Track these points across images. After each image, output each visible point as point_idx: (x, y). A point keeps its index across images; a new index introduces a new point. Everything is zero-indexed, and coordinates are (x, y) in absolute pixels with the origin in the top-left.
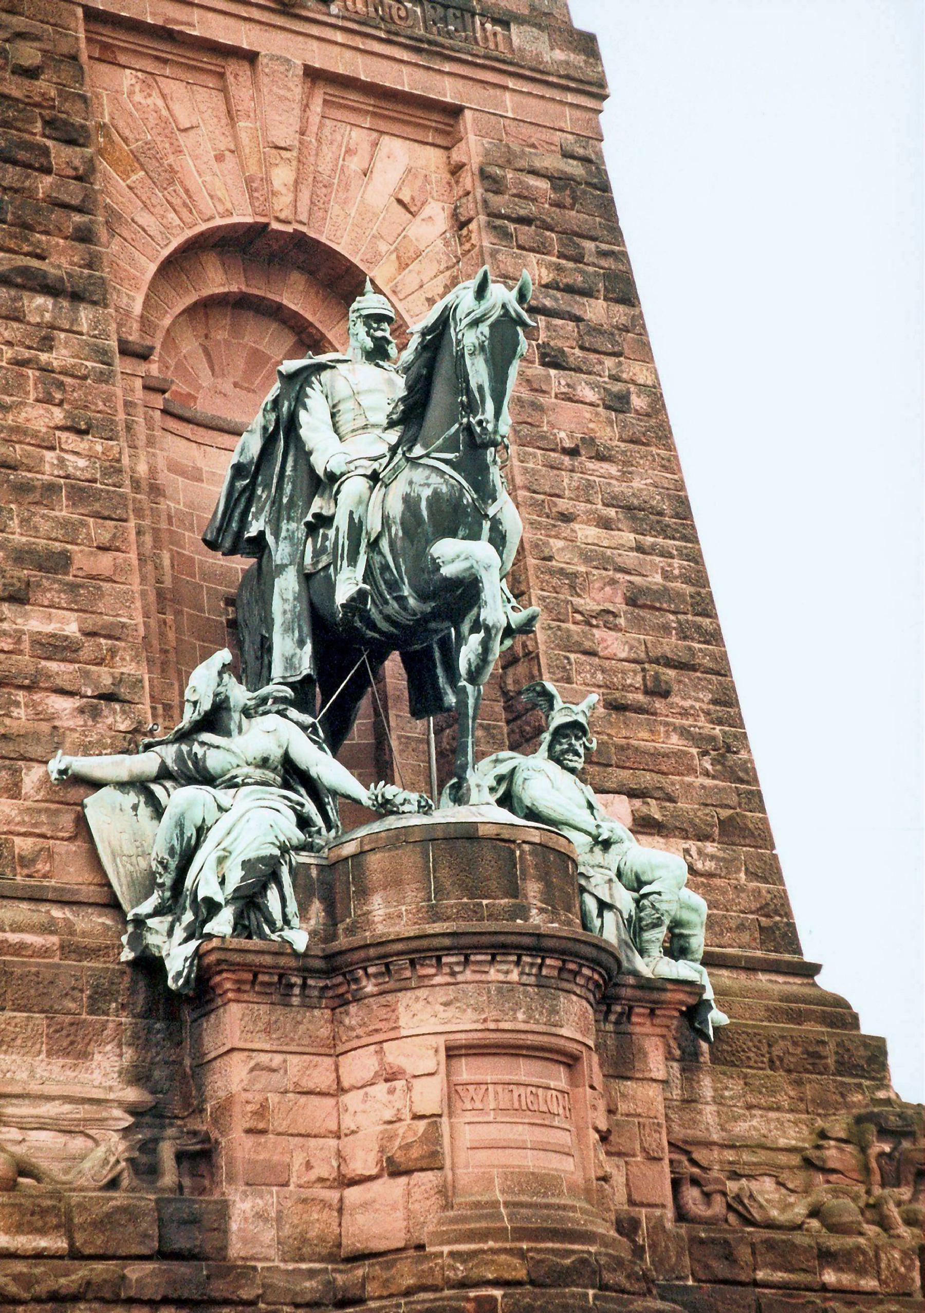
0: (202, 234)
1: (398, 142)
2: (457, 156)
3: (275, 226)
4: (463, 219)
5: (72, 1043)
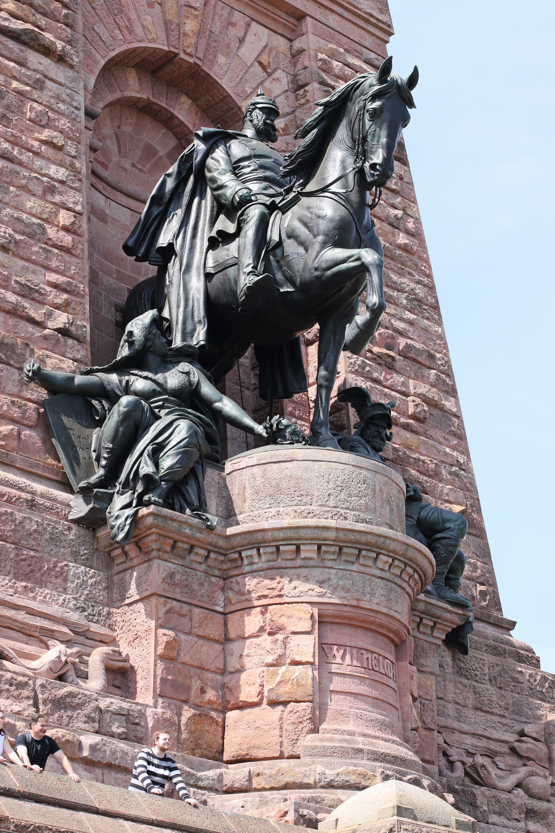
0: (135, 50)
2: (297, 44)
3: (182, 56)
4: (301, 83)
5: (32, 571)
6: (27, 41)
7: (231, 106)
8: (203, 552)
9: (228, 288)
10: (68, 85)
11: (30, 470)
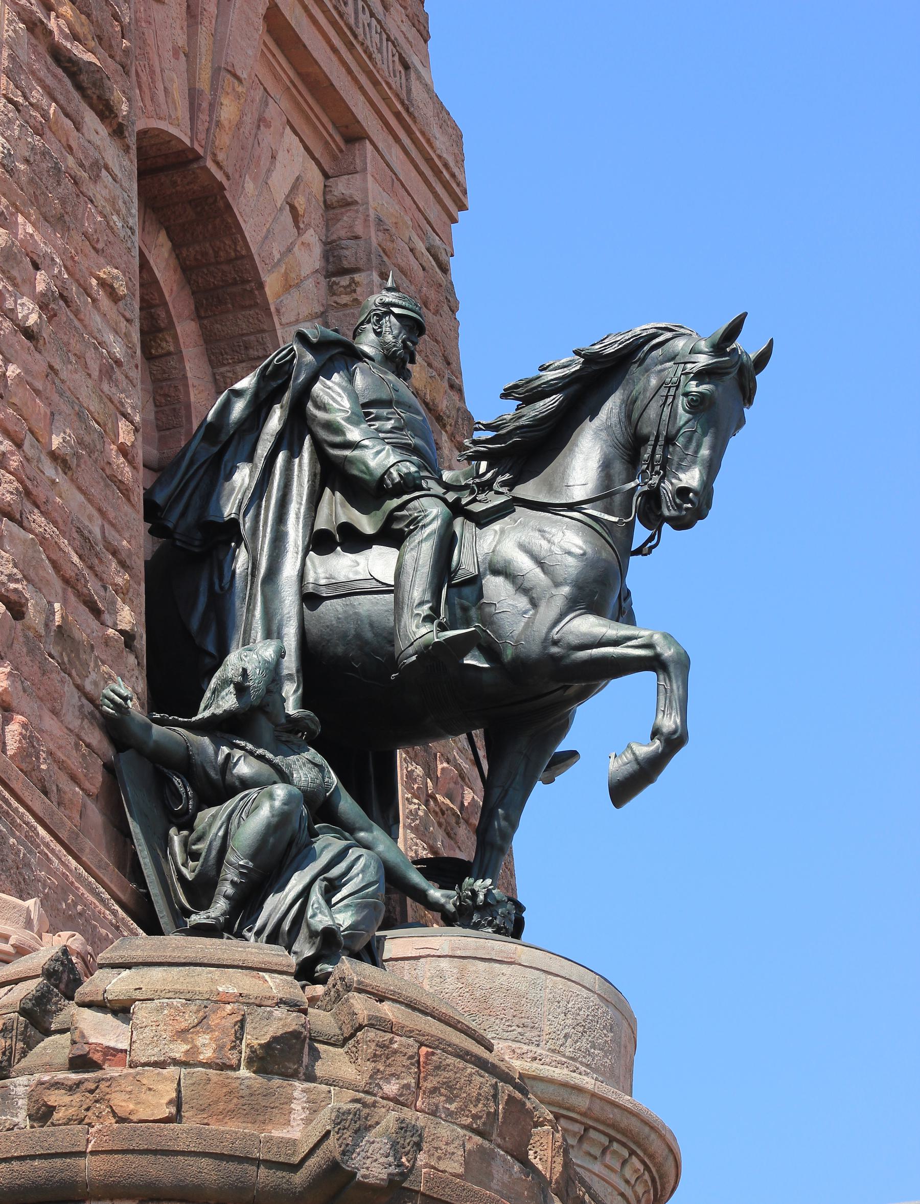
2: (342, 187)
3: (210, 164)
4: (346, 265)
6: (85, 85)
7: (246, 276)
9: (353, 632)
10: (123, 184)
11: (97, 871)
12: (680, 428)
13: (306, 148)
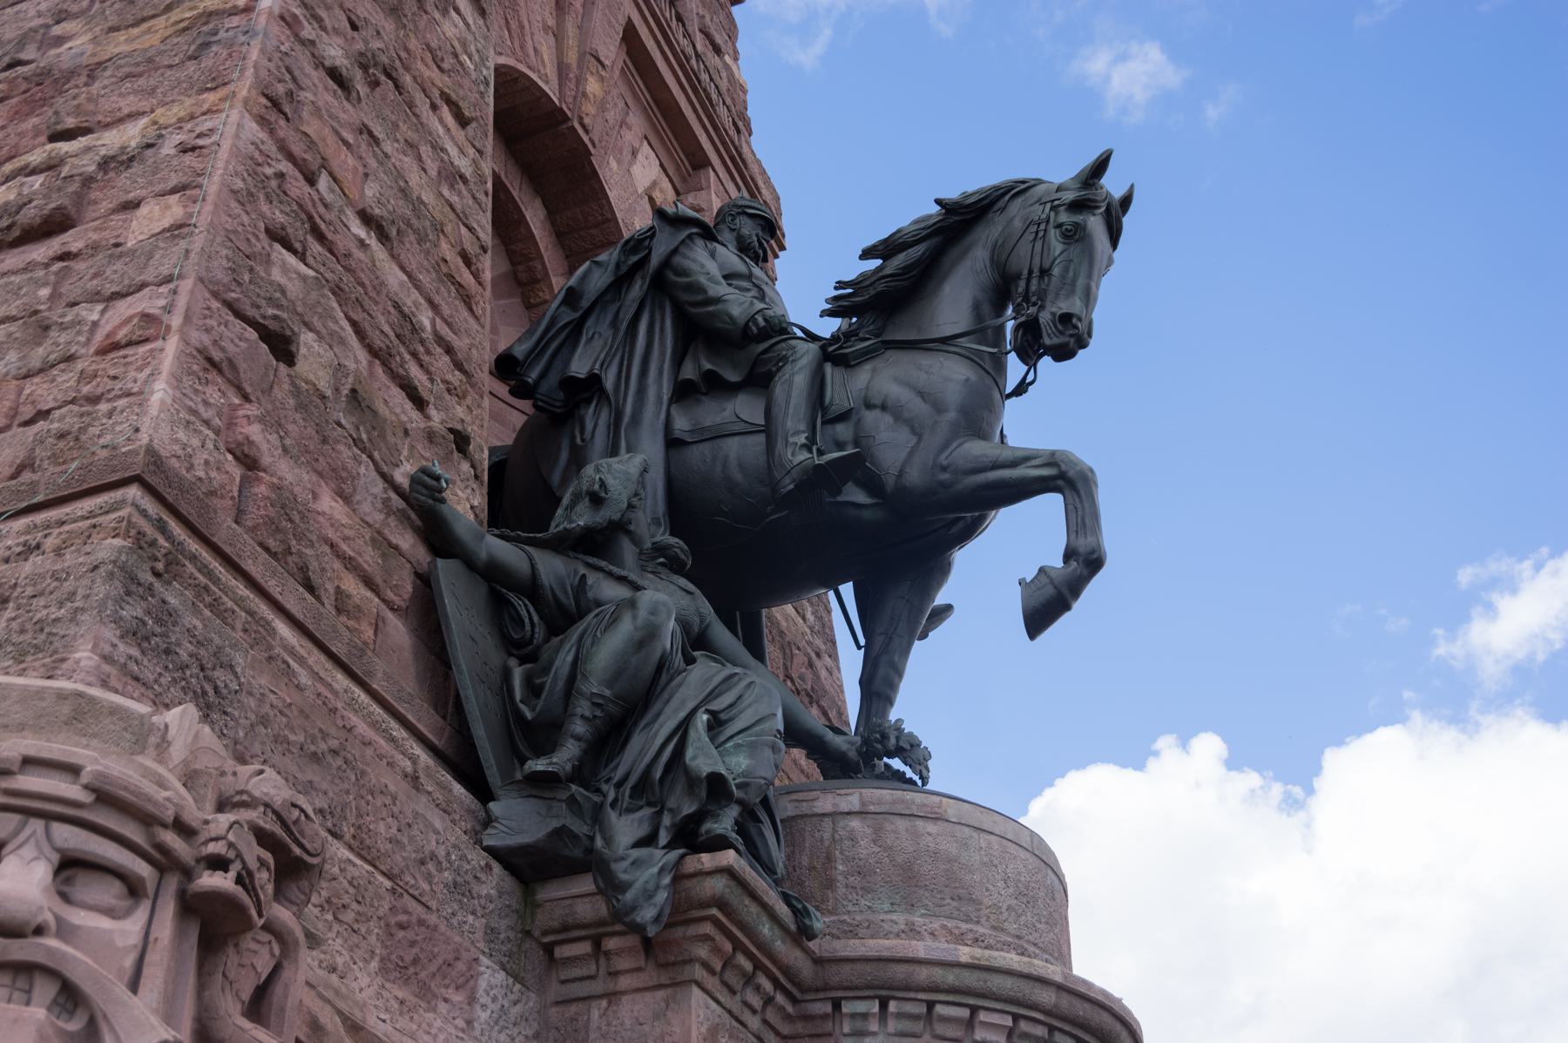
1: (653, 155)
5: (415, 961)
8: (767, 985)
12: (1055, 260)
13: (662, 165)
